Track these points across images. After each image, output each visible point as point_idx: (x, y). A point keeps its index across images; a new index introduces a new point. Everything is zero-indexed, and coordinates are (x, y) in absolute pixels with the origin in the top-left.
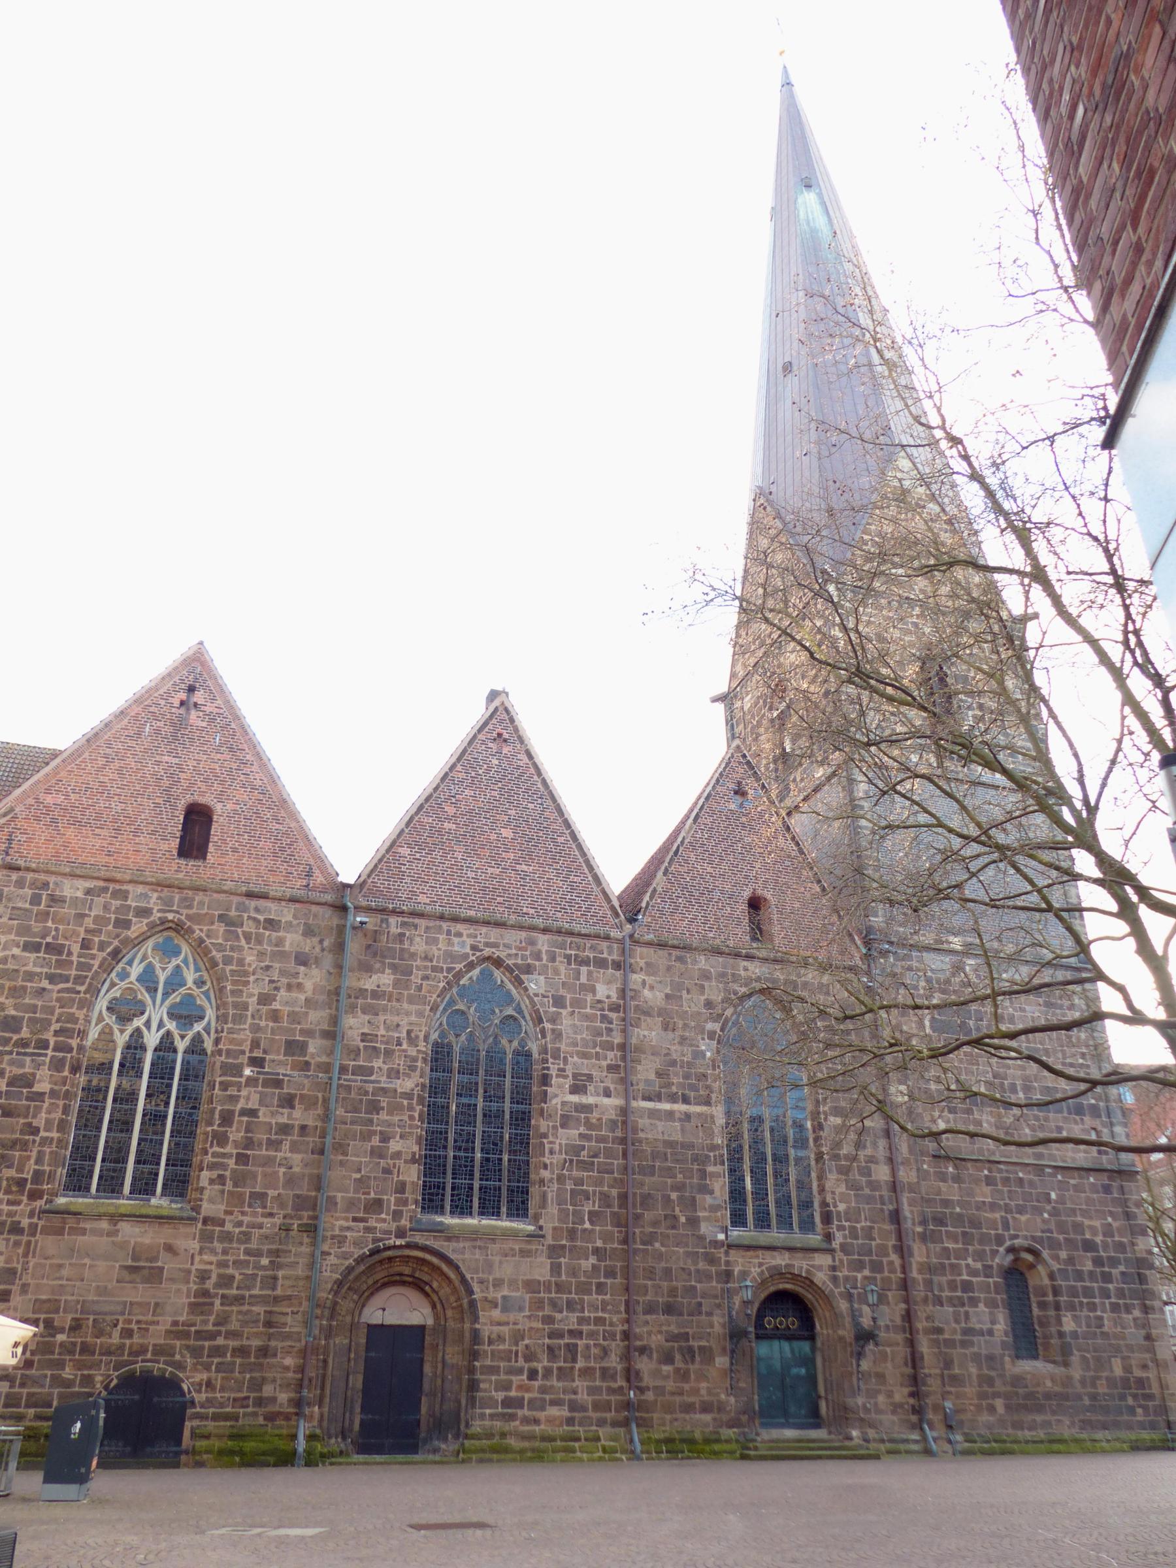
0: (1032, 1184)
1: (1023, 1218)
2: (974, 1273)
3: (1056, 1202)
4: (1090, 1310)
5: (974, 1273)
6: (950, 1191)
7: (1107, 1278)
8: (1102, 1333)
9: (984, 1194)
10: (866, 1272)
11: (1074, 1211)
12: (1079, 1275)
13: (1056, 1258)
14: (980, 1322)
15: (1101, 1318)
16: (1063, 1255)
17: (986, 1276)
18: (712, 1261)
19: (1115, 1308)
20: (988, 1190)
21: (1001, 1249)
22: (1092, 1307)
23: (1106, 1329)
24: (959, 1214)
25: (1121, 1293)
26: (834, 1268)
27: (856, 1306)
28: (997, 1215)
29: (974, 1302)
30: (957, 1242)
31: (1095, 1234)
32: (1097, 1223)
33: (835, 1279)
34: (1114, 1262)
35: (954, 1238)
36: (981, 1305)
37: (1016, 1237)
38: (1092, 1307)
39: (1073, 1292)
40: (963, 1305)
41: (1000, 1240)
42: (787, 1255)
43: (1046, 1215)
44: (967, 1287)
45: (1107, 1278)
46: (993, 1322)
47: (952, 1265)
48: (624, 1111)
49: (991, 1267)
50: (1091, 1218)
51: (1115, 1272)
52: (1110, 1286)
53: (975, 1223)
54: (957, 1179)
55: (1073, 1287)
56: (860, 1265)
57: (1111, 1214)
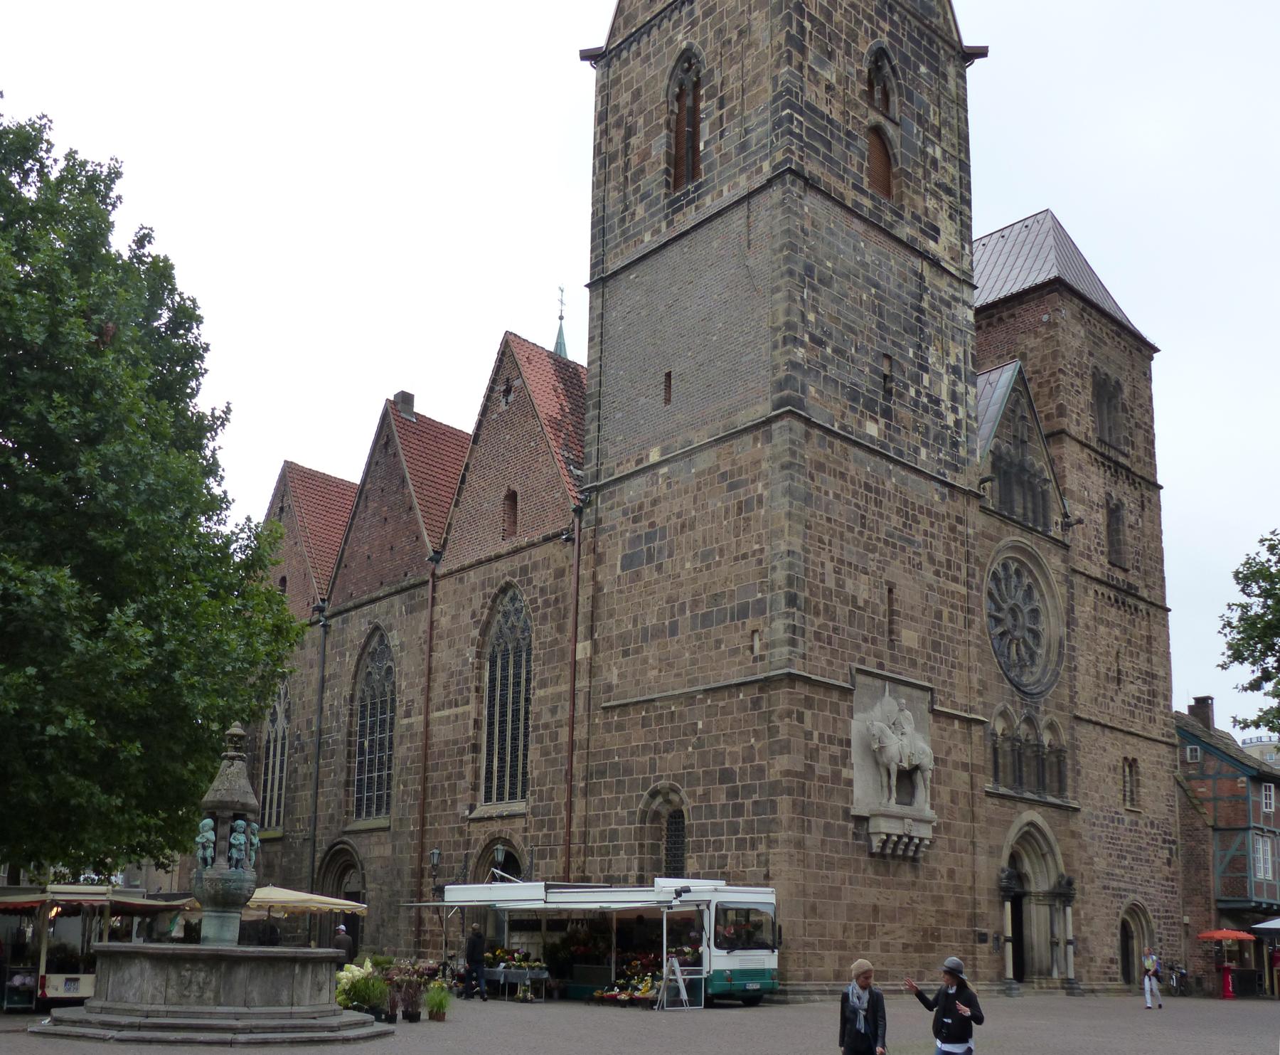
0: (681, 715)
1: (670, 756)
2: (620, 821)
3: (702, 731)
4: (715, 850)
5: (620, 821)
6: (613, 741)
7: (738, 810)
8: (723, 873)
9: (638, 737)
10: (545, 831)
11: (717, 738)
12: (711, 812)
13: (692, 795)
14: (618, 870)
15: (726, 856)
16: (700, 790)
17: (630, 823)
18: (461, 832)
19: (741, 844)
20: (642, 732)
21: (645, 794)
22: (718, 845)
23: (727, 869)
24: (617, 764)
25: (750, 827)
26: (526, 830)
27: (535, 861)
28: (647, 758)
29: (617, 849)
30: (611, 792)
31: (735, 761)
32: (738, 749)
33: (525, 838)
34: (749, 790)
35: (608, 786)
36: (622, 852)
37: (660, 778)
38: (718, 845)
39: (703, 831)
40: (608, 854)
41: (646, 782)
42: (500, 822)
43: (690, 749)
44: (614, 835)
45: (738, 810)
46: (629, 870)
47: (605, 816)
48: (427, 724)
49: (634, 813)
50: (734, 743)
51: (748, 802)
52: (740, 820)
53: (628, 771)
54: (620, 727)
55: (703, 824)
56: (541, 825)
57: (757, 734)
